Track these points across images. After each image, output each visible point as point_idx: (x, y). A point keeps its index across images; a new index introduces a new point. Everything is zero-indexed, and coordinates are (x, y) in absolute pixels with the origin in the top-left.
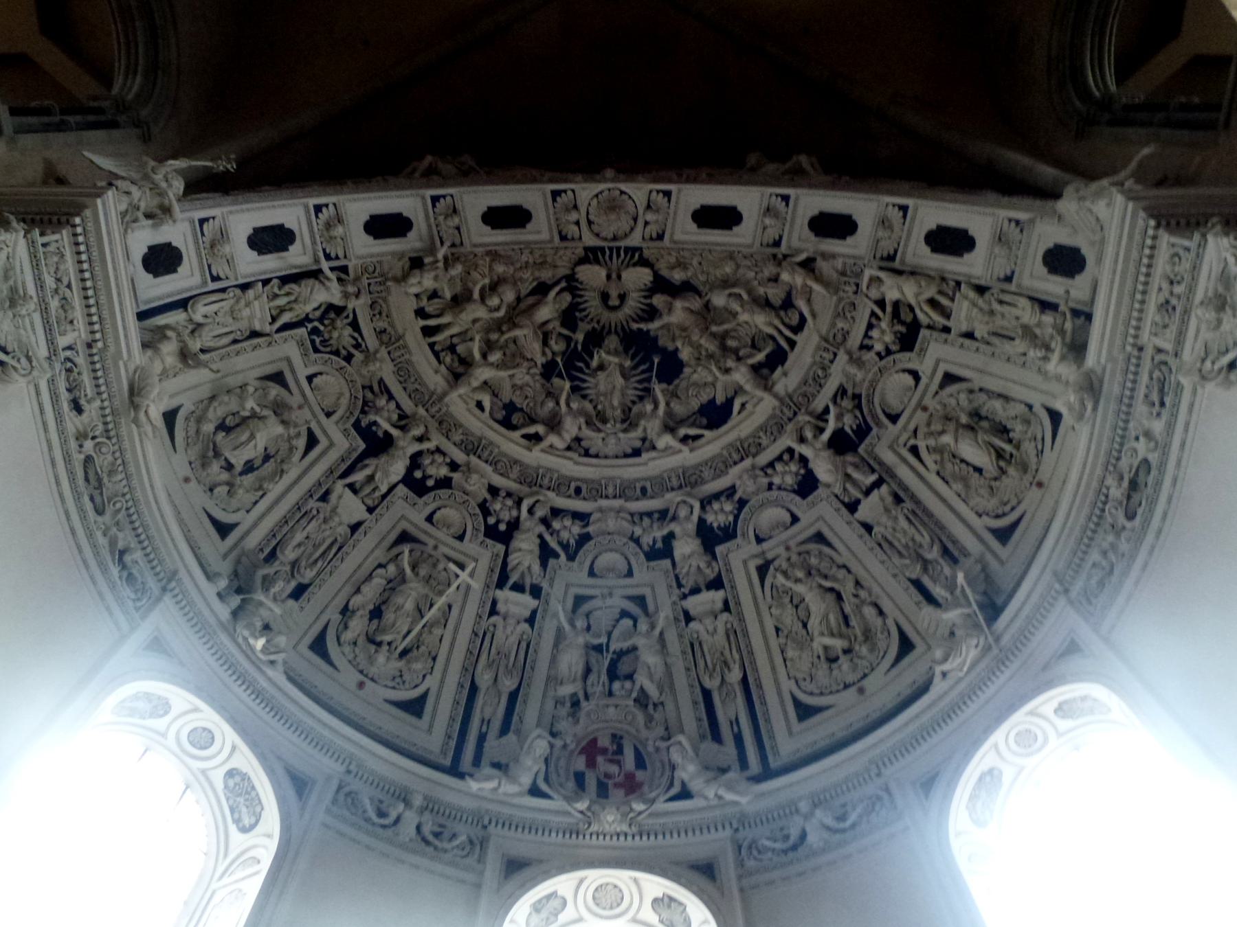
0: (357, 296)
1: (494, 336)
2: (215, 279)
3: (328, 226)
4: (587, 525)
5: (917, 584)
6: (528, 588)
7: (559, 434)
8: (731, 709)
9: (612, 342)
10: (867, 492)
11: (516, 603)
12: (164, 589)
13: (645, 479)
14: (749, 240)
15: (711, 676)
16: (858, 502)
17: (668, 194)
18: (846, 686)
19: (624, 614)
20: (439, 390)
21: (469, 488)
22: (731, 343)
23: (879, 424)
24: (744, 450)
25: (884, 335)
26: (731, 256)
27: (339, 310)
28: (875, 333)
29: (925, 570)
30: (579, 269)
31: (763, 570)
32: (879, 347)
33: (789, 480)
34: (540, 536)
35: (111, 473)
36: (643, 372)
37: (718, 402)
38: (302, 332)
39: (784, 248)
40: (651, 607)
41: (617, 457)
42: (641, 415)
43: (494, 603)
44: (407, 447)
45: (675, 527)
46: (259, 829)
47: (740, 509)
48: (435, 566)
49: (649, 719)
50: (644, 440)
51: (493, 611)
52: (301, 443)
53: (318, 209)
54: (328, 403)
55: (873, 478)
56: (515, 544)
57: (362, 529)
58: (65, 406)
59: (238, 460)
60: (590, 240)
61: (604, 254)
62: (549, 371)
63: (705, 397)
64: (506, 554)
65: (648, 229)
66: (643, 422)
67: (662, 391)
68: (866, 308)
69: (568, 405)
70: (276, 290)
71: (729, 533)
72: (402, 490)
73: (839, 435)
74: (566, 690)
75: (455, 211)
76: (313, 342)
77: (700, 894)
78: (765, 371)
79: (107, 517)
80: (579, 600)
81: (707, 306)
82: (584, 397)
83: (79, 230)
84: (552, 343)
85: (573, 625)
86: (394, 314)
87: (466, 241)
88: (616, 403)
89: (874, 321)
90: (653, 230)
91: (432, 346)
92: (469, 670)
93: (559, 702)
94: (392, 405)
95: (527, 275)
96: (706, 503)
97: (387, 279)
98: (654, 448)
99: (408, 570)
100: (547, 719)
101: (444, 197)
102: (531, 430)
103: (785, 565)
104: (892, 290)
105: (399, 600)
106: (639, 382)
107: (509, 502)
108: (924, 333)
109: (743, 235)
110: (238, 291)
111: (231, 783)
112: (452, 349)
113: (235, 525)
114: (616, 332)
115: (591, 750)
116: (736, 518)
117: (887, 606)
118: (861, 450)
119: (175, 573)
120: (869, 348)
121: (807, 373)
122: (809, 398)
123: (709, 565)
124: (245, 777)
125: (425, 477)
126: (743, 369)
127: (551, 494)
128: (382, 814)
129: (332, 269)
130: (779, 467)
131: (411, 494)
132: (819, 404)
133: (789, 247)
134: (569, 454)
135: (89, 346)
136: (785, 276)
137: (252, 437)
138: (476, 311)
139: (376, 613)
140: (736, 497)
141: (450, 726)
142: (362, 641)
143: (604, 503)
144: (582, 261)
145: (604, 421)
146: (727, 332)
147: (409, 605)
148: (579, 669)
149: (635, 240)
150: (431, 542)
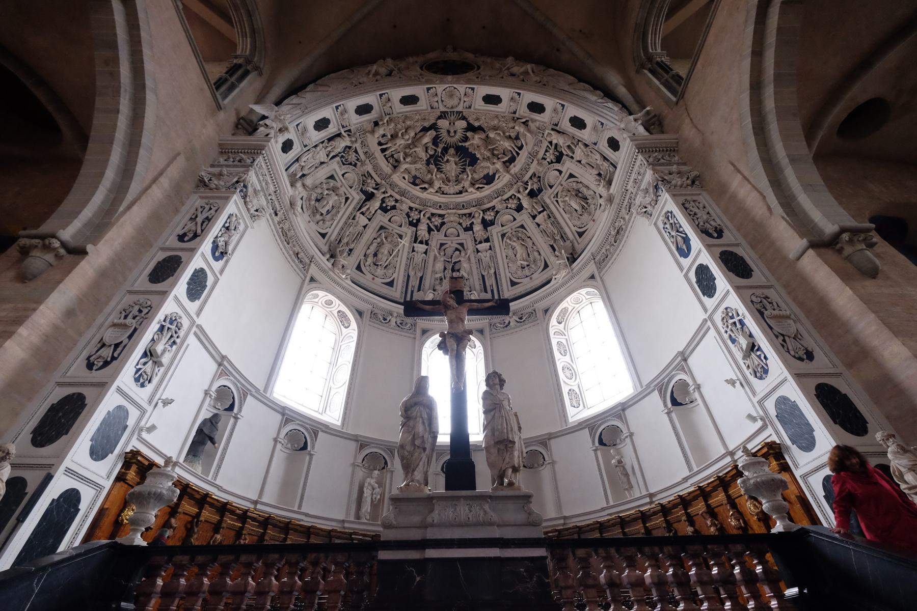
0: (356, 141)
1: (407, 151)
2: (305, 146)
3: (342, 114)
4: (443, 219)
5: (552, 246)
6: (424, 242)
7: (433, 188)
8: (490, 281)
9: (452, 151)
10: (540, 213)
11: (421, 248)
12: (311, 261)
13: (464, 202)
14: (503, 110)
15: (485, 271)
16: (536, 216)
17: (473, 89)
18: (527, 277)
19: (457, 249)
20: (389, 173)
21: (402, 208)
22: (495, 152)
23: (546, 189)
24: (499, 193)
25: (550, 156)
26: (497, 117)
27: (350, 147)
28: (547, 154)
29: (555, 242)
30: (439, 121)
31: (503, 236)
32: (548, 160)
33: (514, 206)
34: (428, 224)
35: (289, 230)
36: (463, 162)
37: (490, 174)
38: (338, 159)
39: (517, 115)
40: (465, 247)
41: (454, 194)
42: (463, 179)
43: (413, 247)
44: (379, 196)
45: (473, 220)
47: (496, 214)
48: (393, 237)
50: (463, 187)
51: (413, 251)
52: (344, 201)
53: (337, 108)
54: (351, 182)
55: (542, 209)
57: (367, 227)
58: (273, 215)
59: (324, 211)
60: (443, 109)
61: (448, 115)
62: (428, 163)
63: (485, 173)
64: (416, 231)
65: (465, 103)
66: (463, 182)
67: (470, 170)
68: (545, 144)
69: (436, 176)
70: (327, 145)
71: (492, 223)
72: (379, 211)
73: (532, 190)
74: (438, 276)
75: (389, 100)
76: (342, 161)
78: (508, 164)
79: (291, 244)
80: (442, 245)
81: (487, 136)
82: (441, 172)
83: (265, 155)
84: (429, 151)
86: (370, 145)
87: (395, 113)
88: (453, 175)
89: (548, 150)
90: (467, 104)
91: (385, 156)
92: (407, 270)
93: (436, 279)
94: (373, 181)
95: (418, 124)
96: (484, 211)
97: (366, 132)
98: (467, 191)
99: (384, 239)
100: (432, 284)
101: (384, 94)
102: (423, 186)
103: (510, 235)
104: (556, 139)
105: (383, 251)
106: (462, 165)
107: (417, 213)
108: (564, 157)
109: (502, 108)
110: (314, 149)
111: (339, 314)
112: (392, 156)
113: (326, 233)
114: (453, 147)
116: (495, 217)
117: (542, 252)
119: (313, 256)
120: (545, 159)
121: (522, 166)
122: (523, 175)
123: (485, 233)
124: (343, 313)
125: (387, 206)
126: (500, 163)
127: (431, 209)
128: (385, 319)
129: (345, 132)
130: (511, 201)
131: (382, 213)
132: (526, 178)
133: (519, 115)
134: (437, 194)
135: (275, 192)
136: (517, 128)
137: (328, 203)
138: (400, 142)
139: (375, 255)
140: (495, 210)
141: (402, 289)
142: (372, 264)
143: (450, 211)
144: (440, 118)
145: (449, 181)
146: (493, 149)
147: (386, 252)
148: (442, 268)
149: (460, 109)
150: (391, 229)
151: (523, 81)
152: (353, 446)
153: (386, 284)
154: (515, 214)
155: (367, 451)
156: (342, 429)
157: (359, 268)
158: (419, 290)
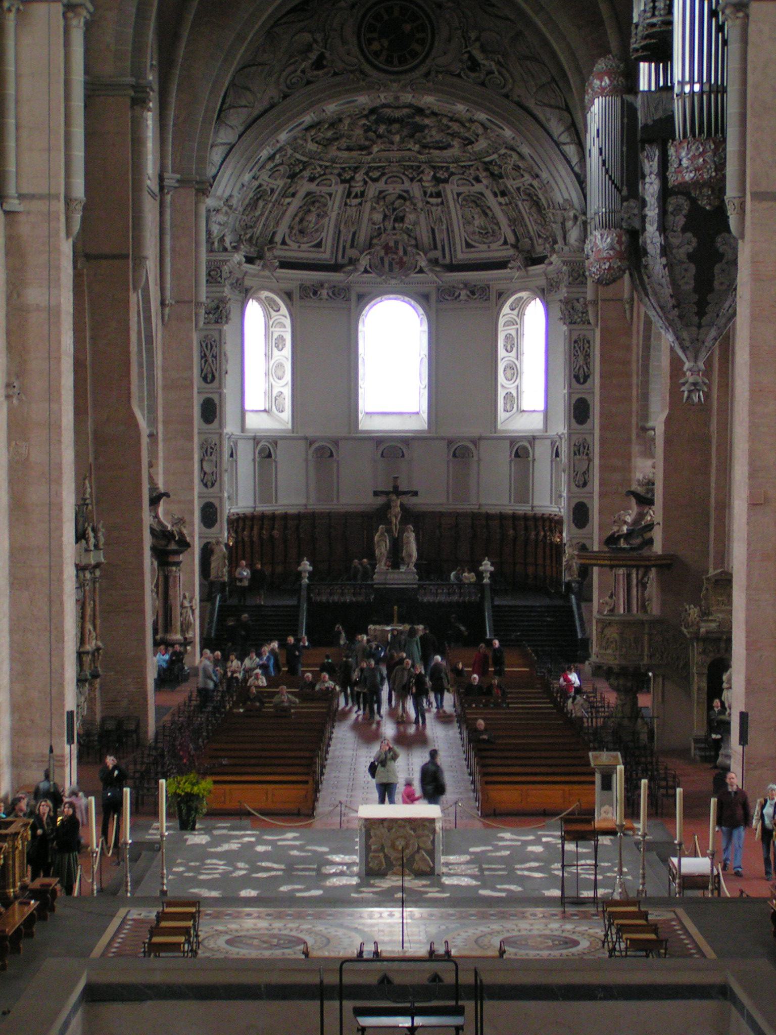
18: (484, 243)
19: (400, 197)
39: (475, 118)
44: (306, 174)
45: (421, 175)
46: (281, 312)
49: (409, 236)
51: (346, 204)
56: (353, 184)
60: (384, 101)
71: (446, 181)
74: (377, 227)
77: (424, 309)
85: (378, 204)
87: (328, 113)
92: (337, 226)
115: (387, 248)
118: (501, 181)
139: (301, 221)
151: (483, 84)
152: (302, 444)
153: (314, 246)
154: (474, 183)
155: (316, 445)
156: (293, 432)
157: (284, 243)
158: (352, 246)
